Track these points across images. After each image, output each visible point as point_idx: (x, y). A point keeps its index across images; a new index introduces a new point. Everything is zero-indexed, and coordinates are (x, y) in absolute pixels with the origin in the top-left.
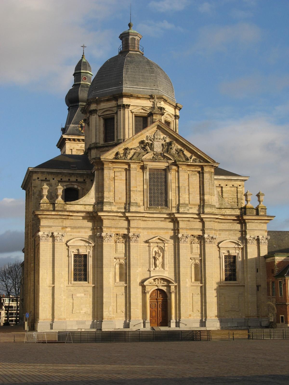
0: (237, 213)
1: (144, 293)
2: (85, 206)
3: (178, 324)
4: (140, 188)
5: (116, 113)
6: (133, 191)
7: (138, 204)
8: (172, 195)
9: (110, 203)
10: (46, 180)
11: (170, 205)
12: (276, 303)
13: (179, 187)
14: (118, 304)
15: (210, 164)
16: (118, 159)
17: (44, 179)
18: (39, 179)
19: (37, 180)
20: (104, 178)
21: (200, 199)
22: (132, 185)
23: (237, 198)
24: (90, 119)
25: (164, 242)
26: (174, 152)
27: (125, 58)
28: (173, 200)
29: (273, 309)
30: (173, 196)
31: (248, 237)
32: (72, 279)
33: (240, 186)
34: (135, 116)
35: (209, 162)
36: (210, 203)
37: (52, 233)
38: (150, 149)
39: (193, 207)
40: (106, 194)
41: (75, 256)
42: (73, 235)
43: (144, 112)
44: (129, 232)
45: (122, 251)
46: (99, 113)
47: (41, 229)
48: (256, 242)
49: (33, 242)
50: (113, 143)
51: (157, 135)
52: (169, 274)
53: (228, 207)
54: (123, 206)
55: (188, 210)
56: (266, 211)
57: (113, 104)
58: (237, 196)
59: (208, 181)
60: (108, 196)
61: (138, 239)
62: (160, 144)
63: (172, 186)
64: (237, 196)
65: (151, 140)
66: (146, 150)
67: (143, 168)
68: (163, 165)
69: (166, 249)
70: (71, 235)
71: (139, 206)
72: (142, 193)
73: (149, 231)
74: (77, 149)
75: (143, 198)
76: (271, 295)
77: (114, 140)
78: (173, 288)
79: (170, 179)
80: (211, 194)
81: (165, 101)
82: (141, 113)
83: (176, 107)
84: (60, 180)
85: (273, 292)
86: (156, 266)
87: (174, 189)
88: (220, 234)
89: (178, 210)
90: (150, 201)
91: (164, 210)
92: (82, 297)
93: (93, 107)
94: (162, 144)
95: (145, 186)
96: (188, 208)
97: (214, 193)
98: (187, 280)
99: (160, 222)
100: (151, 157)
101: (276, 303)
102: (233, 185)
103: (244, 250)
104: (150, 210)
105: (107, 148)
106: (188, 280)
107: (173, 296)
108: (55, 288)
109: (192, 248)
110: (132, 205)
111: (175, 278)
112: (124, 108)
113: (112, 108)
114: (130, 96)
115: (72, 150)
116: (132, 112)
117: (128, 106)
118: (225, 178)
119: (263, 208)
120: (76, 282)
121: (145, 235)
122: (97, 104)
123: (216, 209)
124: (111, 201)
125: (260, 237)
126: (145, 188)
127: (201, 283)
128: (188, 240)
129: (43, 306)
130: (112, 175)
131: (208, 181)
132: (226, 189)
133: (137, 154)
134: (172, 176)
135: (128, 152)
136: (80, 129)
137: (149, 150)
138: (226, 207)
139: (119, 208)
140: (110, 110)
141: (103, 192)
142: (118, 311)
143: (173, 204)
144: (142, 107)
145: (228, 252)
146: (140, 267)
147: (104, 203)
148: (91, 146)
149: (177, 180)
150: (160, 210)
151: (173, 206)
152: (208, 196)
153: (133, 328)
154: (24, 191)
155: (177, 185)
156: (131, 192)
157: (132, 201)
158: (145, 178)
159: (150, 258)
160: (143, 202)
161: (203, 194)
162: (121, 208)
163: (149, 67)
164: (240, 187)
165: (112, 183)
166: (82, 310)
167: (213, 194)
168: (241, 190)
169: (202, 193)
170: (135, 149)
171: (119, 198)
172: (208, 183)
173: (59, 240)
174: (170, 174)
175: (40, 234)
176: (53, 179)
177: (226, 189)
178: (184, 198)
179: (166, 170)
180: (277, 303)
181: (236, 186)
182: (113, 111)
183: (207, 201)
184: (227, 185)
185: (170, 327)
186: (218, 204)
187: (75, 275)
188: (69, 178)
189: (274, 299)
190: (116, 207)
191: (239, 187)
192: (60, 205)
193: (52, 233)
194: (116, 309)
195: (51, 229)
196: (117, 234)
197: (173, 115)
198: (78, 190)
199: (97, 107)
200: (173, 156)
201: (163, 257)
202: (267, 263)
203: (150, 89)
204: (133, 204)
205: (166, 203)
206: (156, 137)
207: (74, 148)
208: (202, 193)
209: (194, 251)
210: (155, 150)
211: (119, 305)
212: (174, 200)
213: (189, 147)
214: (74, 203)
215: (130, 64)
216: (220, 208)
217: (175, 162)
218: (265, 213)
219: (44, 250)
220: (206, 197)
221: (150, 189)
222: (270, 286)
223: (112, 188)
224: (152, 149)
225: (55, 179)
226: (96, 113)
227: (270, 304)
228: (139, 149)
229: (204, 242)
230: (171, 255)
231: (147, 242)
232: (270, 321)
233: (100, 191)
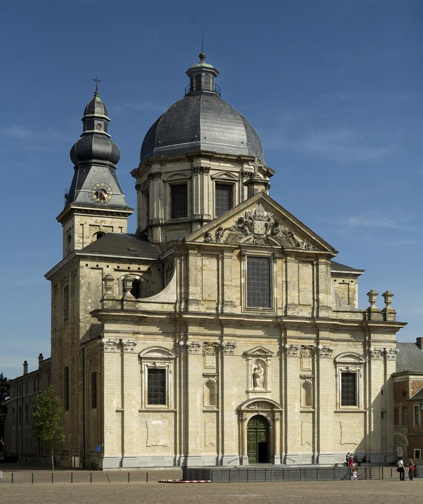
0: (359, 319)
1: (241, 420)
2: (162, 305)
3: (283, 460)
4: (237, 282)
5: (191, 178)
6: (226, 285)
7: (233, 304)
8: (277, 293)
9: (197, 302)
10: (97, 268)
11: (274, 306)
12: (408, 433)
13: (286, 282)
14: (206, 434)
15: (327, 253)
16: (208, 242)
17: (95, 266)
18: (89, 266)
19: (86, 267)
20: (190, 267)
21: (313, 298)
22: (225, 278)
23: (349, 298)
24: (151, 185)
25: (267, 354)
26: (281, 235)
27: (200, 102)
28: (278, 299)
29: (404, 441)
30: (278, 293)
31: (372, 349)
32: (147, 402)
33: (352, 282)
34: (216, 184)
35: (327, 250)
36: (326, 304)
37: (121, 340)
38: (250, 231)
39: (304, 308)
40: (192, 289)
41: (150, 371)
42: (147, 343)
43: (228, 178)
44: (222, 341)
45: (212, 365)
46: (164, 177)
47: (105, 335)
48: (382, 358)
49: (82, 352)
50: (185, 220)
51: (259, 211)
52: (273, 396)
53: (347, 310)
54: (214, 305)
55: (298, 313)
56: (395, 317)
57: (186, 165)
58: (349, 295)
59: (324, 275)
60: (194, 292)
61: (234, 350)
62: (263, 223)
63: (278, 280)
64: (349, 295)
65: (250, 218)
66: (245, 231)
67: (241, 257)
68: (266, 253)
70: (145, 343)
71: (235, 306)
72: (239, 289)
73: (247, 339)
74: (90, 225)
75: (240, 295)
76: (400, 423)
77: (185, 215)
78: (277, 416)
79: (275, 271)
80: (327, 292)
84: (116, 268)
85: (403, 419)
86: (255, 385)
87: (279, 284)
88: (336, 345)
89: (286, 312)
90: (249, 299)
91: (266, 312)
92: (158, 426)
93: (156, 168)
94: (266, 225)
95: (242, 279)
96: (297, 310)
97: (330, 291)
98: (296, 404)
100: (251, 241)
101: (408, 433)
102: (343, 281)
103: (367, 366)
104: (249, 311)
105: (176, 226)
106: (297, 404)
107: (278, 424)
108: (125, 413)
109: (301, 363)
110: (227, 305)
111: (281, 401)
112: (201, 172)
113: (186, 171)
114: (211, 156)
115: (83, 225)
116: (212, 179)
117: (207, 169)
119: (392, 312)
120: (151, 406)
121: (243, 345)
122: (161, 165)
123: (332, 312)
124: (198, 299)
125: (388, 350)
126: (242, 282)
127: (314, 408)
128: (298, 352)
129: (109, 437)
130: (199, 263)
131: (324, 275)
133: (232, 237)
134: (277, 267)
135: (221, 232)
136: (95, 197)
137: (249, 232)
138: (345, 310)
139: (208, 309)
140: (180, 174)
141: (187, 286)
142: (207, 443)
143: (278, 304)
144: (226, 171)
145: (347, 368)
146: (236, 387)
147: (190, 302)
148: (153, 223)
149: (284, 273)
150: (261, 312)
151: (278, 307)
152: (324, 294)
153: (226, 465)
154: (49, 282)
155: (284, 279)
156: (225, 287)
157: (226, 299)
158: (242, 269)
159: (248, 375)
160: (240, 301)
161: (318, 293)
162: (211, 309)
163: (235, 117)
164: (352, 284)
165: (199, 274)
166: (159, 442)
168: (353, 287)
169: (316, 290)
170: (230, 230)
171: (209, 294)
172: (324, 277)
173: (129, 350)
174: (275, 264)
175: (104, 340)
176: (108, 267)
178: (293, 297)
179: (269, 260)
180: (410, 434)
181: (347, 282)
182: (185, 175)
183: (322, 302)
184: (335, 281)
185: (274, 464)
186: (335, 305)
187: (149, 396)
188: (129, 265)
189: (406, 429)
190: (205, 307)
191: (351, 283)
192: (130, 302)
193: (121, 340)
194: (204, 440)
195: (119, 335)
196: (206, 343)
198: (141, 282)
199: (161, 169)
200: (280, 241)
201: (265, 374)
202: (394, 383)
203: (236, 147)
204: (227, 303)
205: (268, 301)
206: (257, 214)
207: (85, 223)
208: (316, 290)
209: (304, 367)
210: (256, 232)
211: (208, 436)
213: (300, 229)
214: (148, 301)
215: (209, 111)
216: (337, 312)
217: (283, 248)
218: (394, 319)
219: (109, 363)
220: (321, 296)
221: (249, 284)
222: (400, 412)
223: (199, 282)
224: (252, 230)
225: (110, 267)
226: (160, 177)
227: (397, 435)
228: (235, 230)
229: (318, 356)
230: (275, 372)
231: (245, 355)
232: (398, 456)
233: (185, 283)
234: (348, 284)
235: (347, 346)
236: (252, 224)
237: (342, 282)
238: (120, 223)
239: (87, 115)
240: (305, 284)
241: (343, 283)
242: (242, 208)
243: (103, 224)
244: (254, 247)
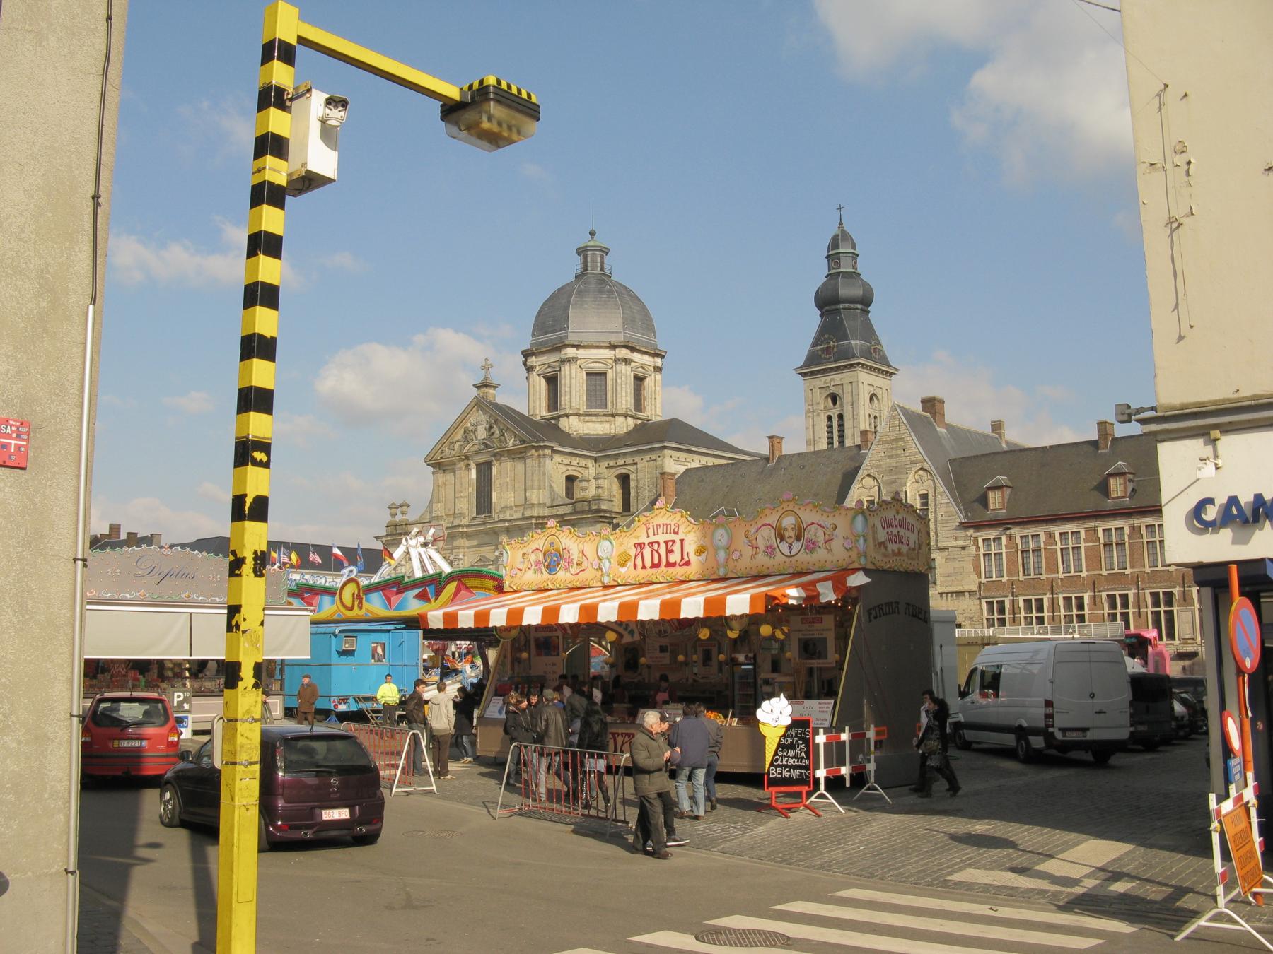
6: (458, 497)
8: (494, 498)
16: (441, 458)
33: (659, 457)
68: (484, 458)
71: (464, 518)
81: (578, 347)
83: (613, 347)
97: (545, 486)
118: (636, 449)
132: (642, 465)
167: (542, 486)
168: (660, 463)
177: (642, 465)
197: (612, 359)
234: (655, 460)
236: (476, 430)
237: (648, 459)
238: (851, 377)
239: (830, 253)
241: (651, 460)
243: (833, 384)
244: (476, 453)
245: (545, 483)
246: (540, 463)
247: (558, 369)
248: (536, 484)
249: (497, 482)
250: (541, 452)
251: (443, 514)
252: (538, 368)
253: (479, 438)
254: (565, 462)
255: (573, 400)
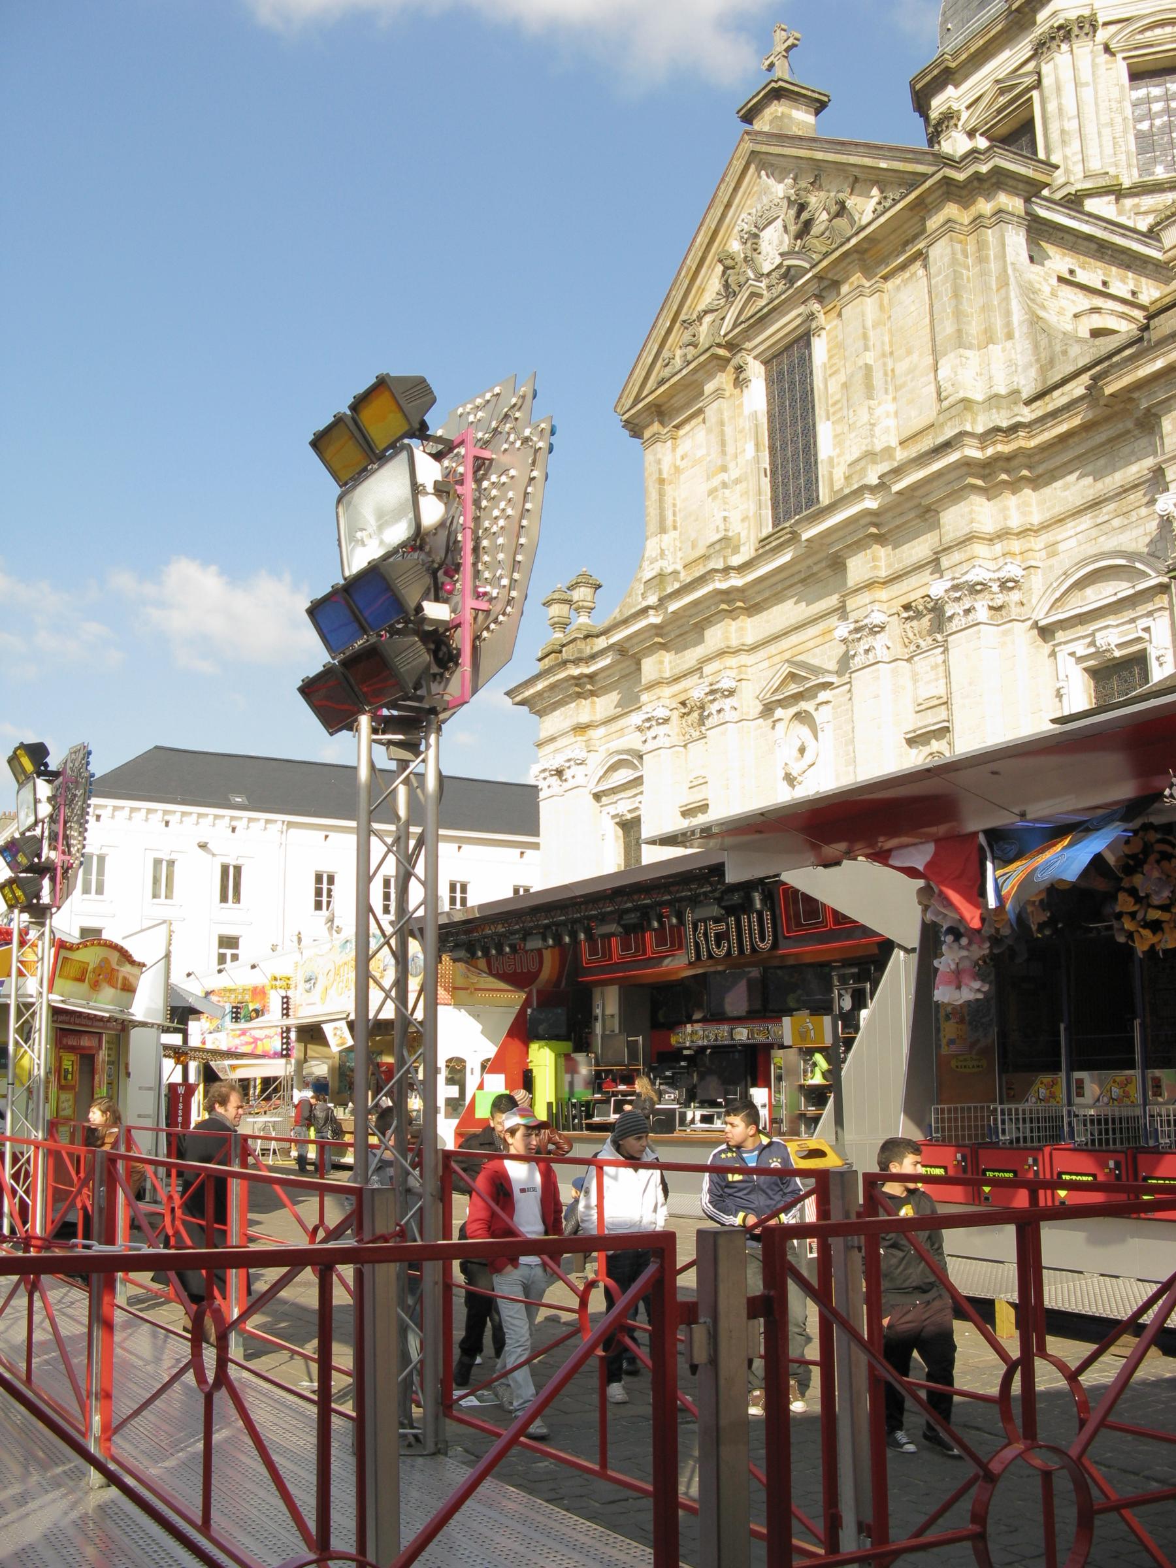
35: (926, 177)
69: (821, 716)
71: (736, 550)
82: (999, 111)
97: (1008, 324)
99: (800, 587)
134: (820, 348)
212: (839, 456)
235: (1094, 532)
240: (909, 352)
242: (713, 227)
245: (1008, 313)
246: (981, 246)
247: (1028, 81)
248: (974, 328)
249: (834, 386)
250: (984, 206)
251: (679, 567)
252: (965, 115)
253: (766, 269)
254: (1082, 277)
255: (1093, 150)
